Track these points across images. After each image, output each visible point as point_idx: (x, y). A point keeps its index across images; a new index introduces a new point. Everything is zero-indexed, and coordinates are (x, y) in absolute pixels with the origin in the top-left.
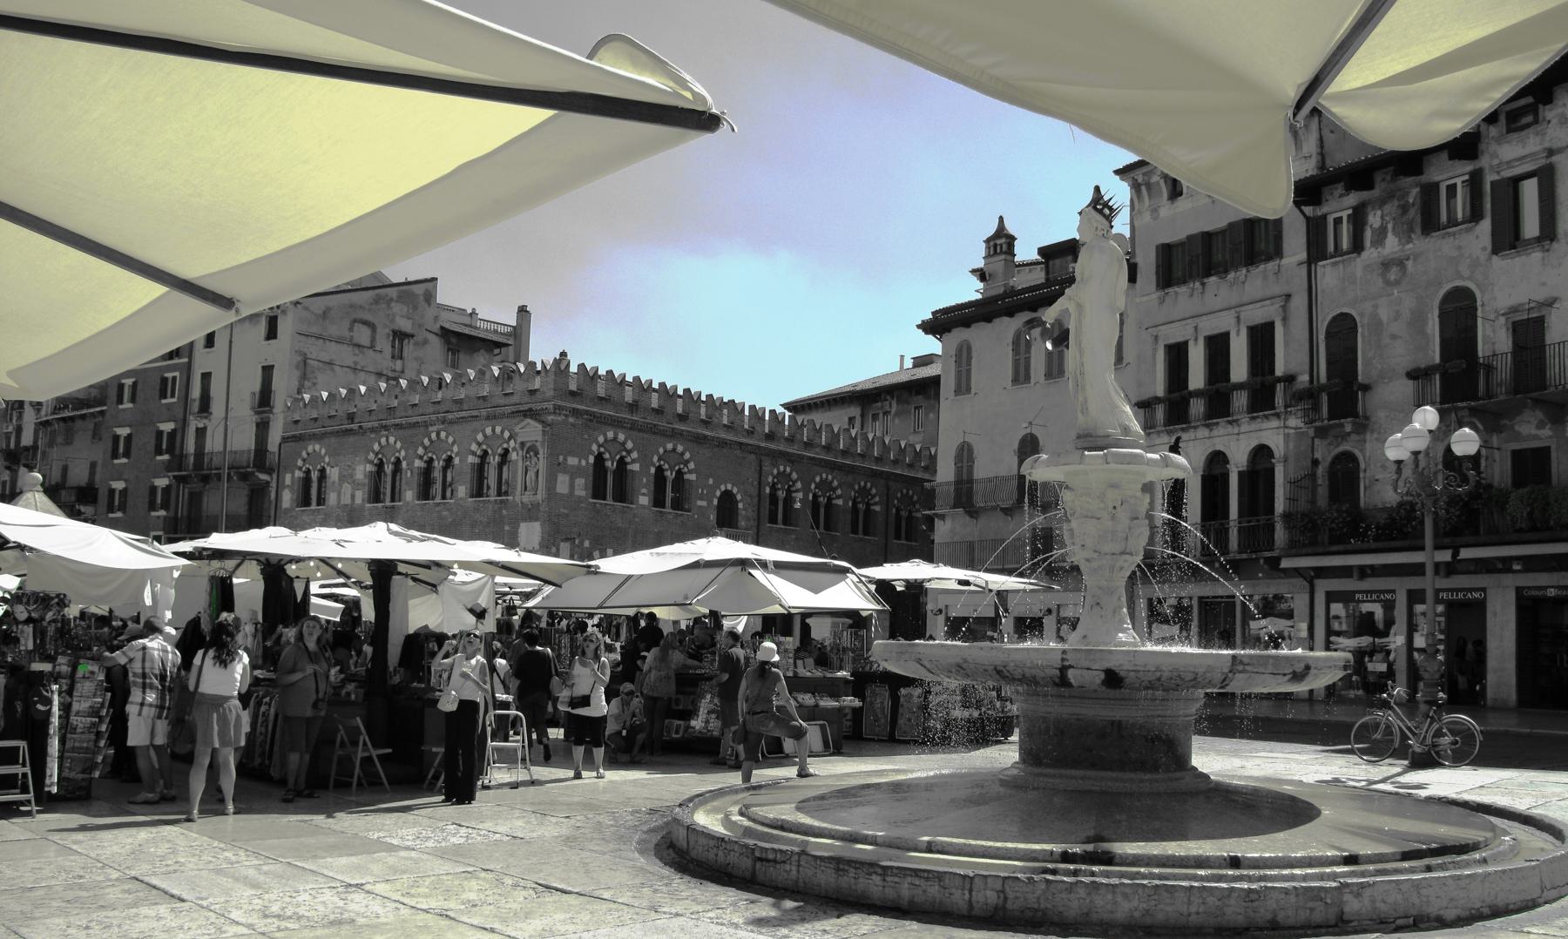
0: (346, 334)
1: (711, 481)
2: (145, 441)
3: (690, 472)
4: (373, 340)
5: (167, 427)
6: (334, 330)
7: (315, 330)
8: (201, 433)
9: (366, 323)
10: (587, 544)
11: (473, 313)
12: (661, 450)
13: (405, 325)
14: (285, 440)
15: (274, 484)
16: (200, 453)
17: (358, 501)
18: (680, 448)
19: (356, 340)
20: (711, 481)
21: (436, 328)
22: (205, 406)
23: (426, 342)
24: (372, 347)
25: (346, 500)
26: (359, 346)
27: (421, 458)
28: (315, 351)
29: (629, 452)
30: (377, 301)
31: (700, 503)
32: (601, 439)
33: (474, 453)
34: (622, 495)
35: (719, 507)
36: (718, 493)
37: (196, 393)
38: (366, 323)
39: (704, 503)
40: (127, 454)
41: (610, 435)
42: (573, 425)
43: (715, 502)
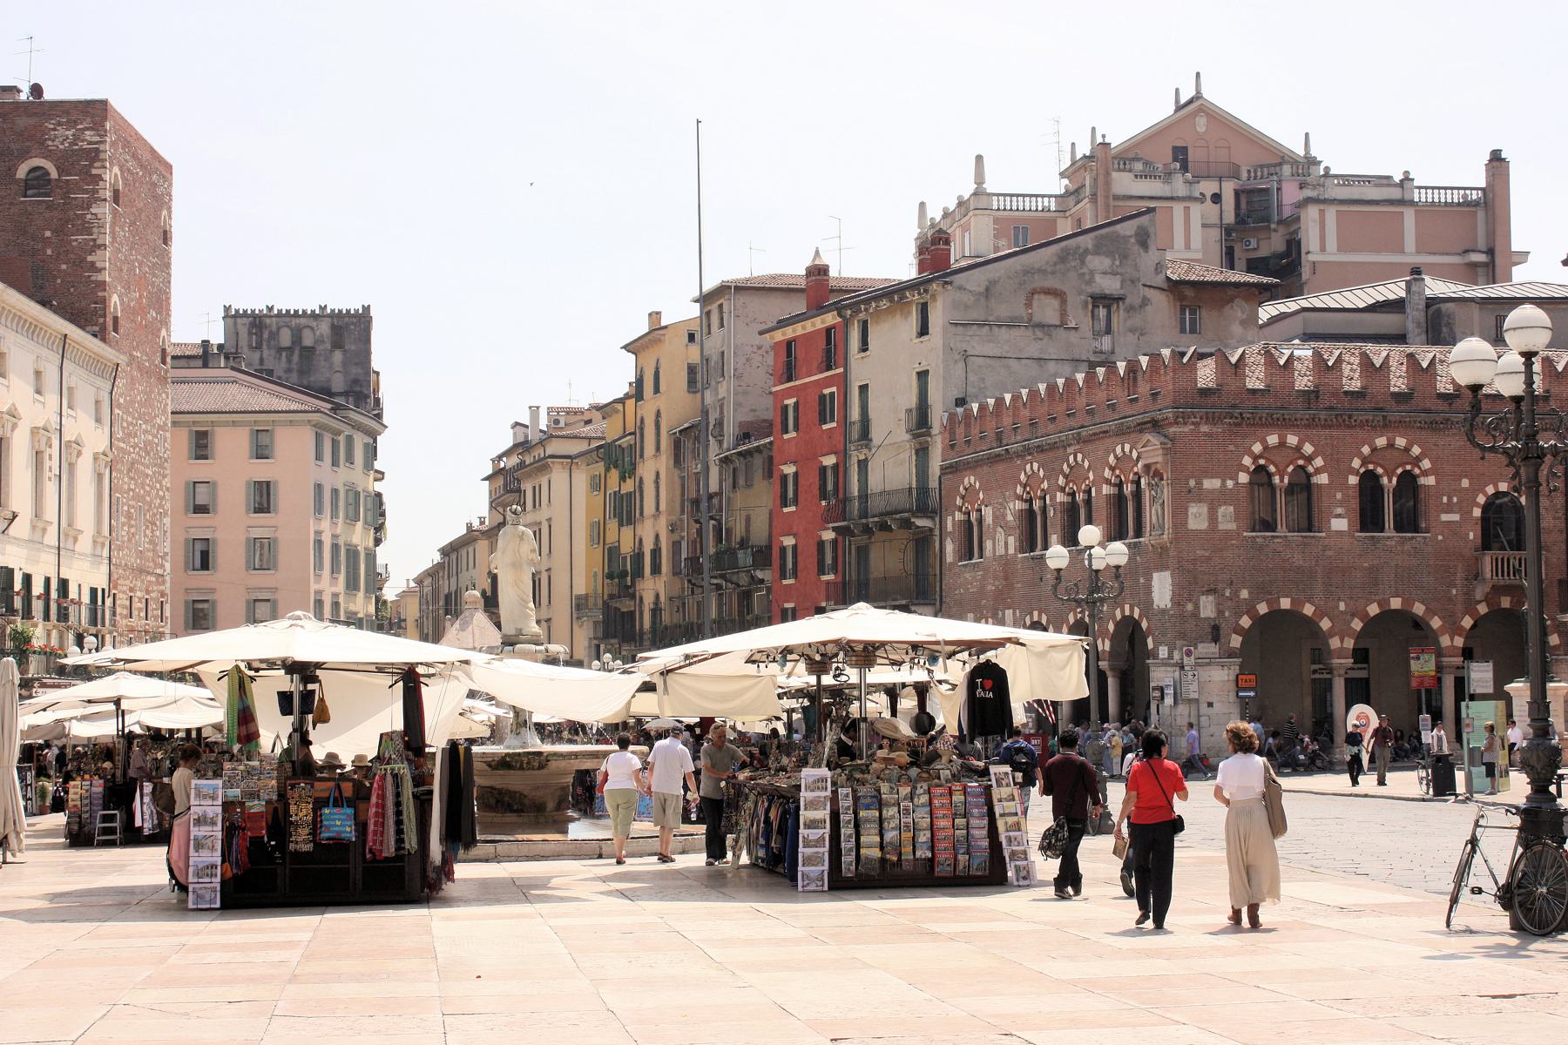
0: (1021, 311)
1: (1465, 483)
2: (811, 481)
3: (1425, 473)
4: (1063, 314)
5: (829, 461)
6: (1003, 310)
7: (975, 314)
8: (863, 464)
9: (1048, 292)
10: (1244, 594)
11: (1407, 178)
12: (1366, 450)
13: (1111, 285)
14: (949, 470)
15: (937, 532)
16: (864, 496)
17: (1011, 551)
18: (1401, 442)
19: (1036, 319)
20: (1465, 483)
21: (1159, 281)
22: (865, 434)
23: (1145, 302)
24: (1062, 324)
25: (1001, 551)
26: (1041, 326)
27: (1063, 490)
28: (978, 345)
29: (1309, 459)
30: (1063, 258)
31: (1445, 517)
32: (1257, 448)
33: (1108, 482)
34: (1309, 522)
35: (1484, 519)
36: (1481, 499)
37: (855, 414)
38: (1048, 292)
39: (1455, 517)
40: (796, 502)
41: (1273, 439)
42: (1206, 434)
43: (1477, 512)
